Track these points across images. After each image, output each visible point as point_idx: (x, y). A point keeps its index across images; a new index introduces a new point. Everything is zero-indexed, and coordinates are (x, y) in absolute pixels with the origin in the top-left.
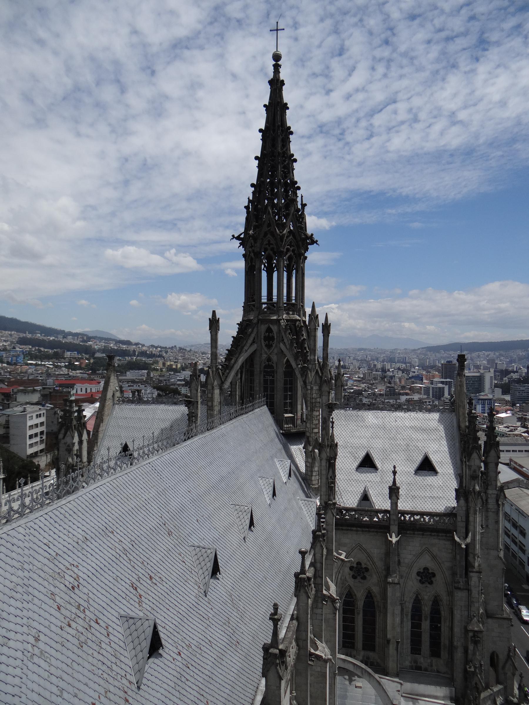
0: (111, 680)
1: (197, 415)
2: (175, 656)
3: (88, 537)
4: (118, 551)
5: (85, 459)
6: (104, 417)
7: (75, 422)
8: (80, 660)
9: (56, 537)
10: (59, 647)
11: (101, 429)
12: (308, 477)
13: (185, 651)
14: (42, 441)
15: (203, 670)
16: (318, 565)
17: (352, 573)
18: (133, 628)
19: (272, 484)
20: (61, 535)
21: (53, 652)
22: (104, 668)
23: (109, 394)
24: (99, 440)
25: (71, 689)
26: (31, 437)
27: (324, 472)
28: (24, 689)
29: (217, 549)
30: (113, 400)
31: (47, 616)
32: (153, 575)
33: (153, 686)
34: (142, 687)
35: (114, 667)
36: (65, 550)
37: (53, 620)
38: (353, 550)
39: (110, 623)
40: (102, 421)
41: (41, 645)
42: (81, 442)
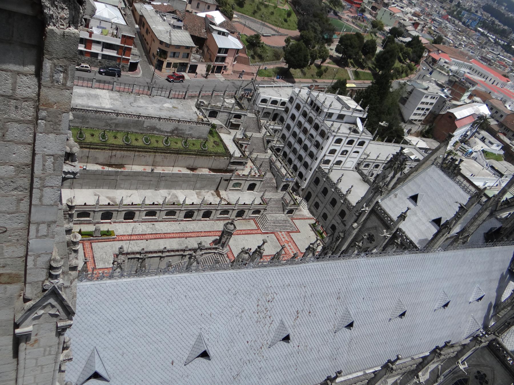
0: (260, 339)
1: (461, 217)
2: (296, 346)
3: (291, 285)
4: (301, 295)
5: (390, 186)
6: (420, 170)
7: (396, 166)
8: (253, 326)
9: (276, 279)
10: (248, 318)
11: (412, 174)
12: (500, 308)
13: (302, 347)
14: (424, 115)
15: (305, 358)
16: (426, 362)
17: (476, 374)
18: (282, 328)
19: (446, 302)
20: (279, 280)
21: (245, 318)
22: (261, 333)
23: (433, 158)
24: (407, 180)
25: (243, 333)
26: (419, 109)
27: (507, 316)
28: (228, 324)
29: (355, 321)
30: (434, 162)
31: (252, 306)
32: (311, 311)
33: (277, 350)
34: (271, 348)
35: (265, 335)
36: (276, 286)
37: (253, 308)
38: (487, 366)
39: (275, 320)
40: (416, 170)
41: (243, 314)
42: (393, 177)
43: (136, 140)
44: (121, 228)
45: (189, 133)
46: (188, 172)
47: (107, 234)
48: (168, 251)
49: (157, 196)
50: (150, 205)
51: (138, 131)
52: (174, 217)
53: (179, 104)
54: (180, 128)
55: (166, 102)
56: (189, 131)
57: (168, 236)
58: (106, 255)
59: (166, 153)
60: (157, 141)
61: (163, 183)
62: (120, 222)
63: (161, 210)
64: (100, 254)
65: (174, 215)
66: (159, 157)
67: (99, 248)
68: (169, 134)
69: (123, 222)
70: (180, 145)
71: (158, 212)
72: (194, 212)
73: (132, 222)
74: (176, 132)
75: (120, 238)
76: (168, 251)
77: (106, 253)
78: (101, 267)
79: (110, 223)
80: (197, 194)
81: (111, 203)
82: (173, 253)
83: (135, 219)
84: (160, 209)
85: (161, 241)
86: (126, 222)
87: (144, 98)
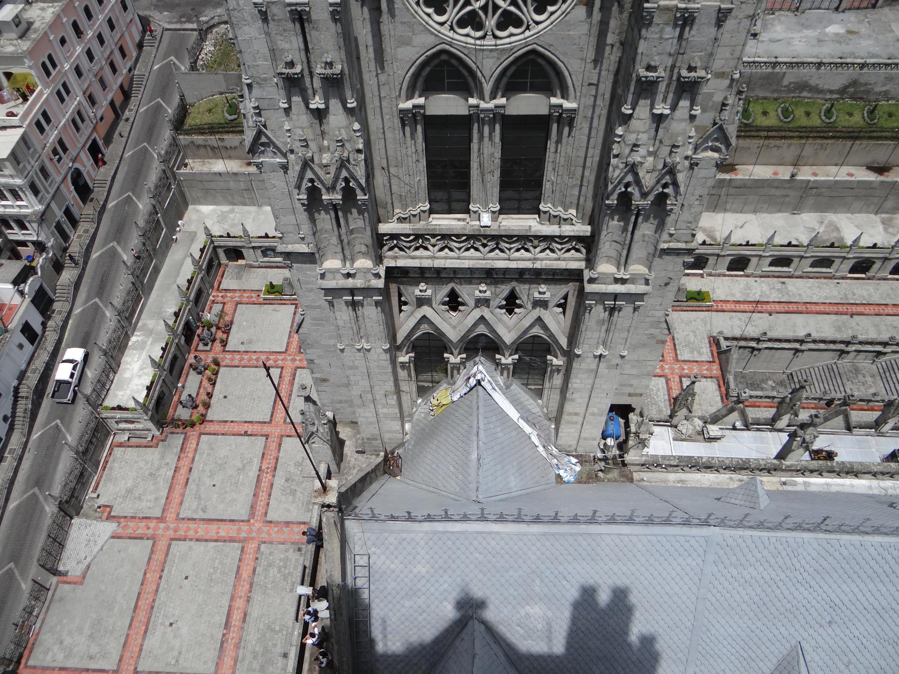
43: (765, 113)
44: (722, 286)
45: (883, 89)
46: (872, 177)
47: (698, 297)
48: (814, 341)
49: (798, 228)
50: (782, 246)
51: (768, 95)
52: (828, 270)
53: (861, 22)
54: (862, 81)
55: (831, 22)
56: (884, 85)
57: (813, 308)
58: (695, 336)
59: (826, 138)
60: (808, 114)
61: (811, 201)
62: (719, 275)
63: (802, 257)
64: (685, 333)
65: (829, 267)
66: (810, 148)
67: (682, 321)
68: (835, 96)
69: (725, 275)
70: (857, 119)
71: (796, 260)
72: (874, 263)
73: (741, 276)
74: (854, 91)
75: (720, 307)
76: (814, 341)
77: (694, 332)
78: (686, 359)
79: (702, 276)
80: (883, 223)
81: (708, 241)
82: (822, 346)
83: (749, 271)
84: (802, 254)
85: (799, 319)
86: (731, 276)
87: (783, 18)
